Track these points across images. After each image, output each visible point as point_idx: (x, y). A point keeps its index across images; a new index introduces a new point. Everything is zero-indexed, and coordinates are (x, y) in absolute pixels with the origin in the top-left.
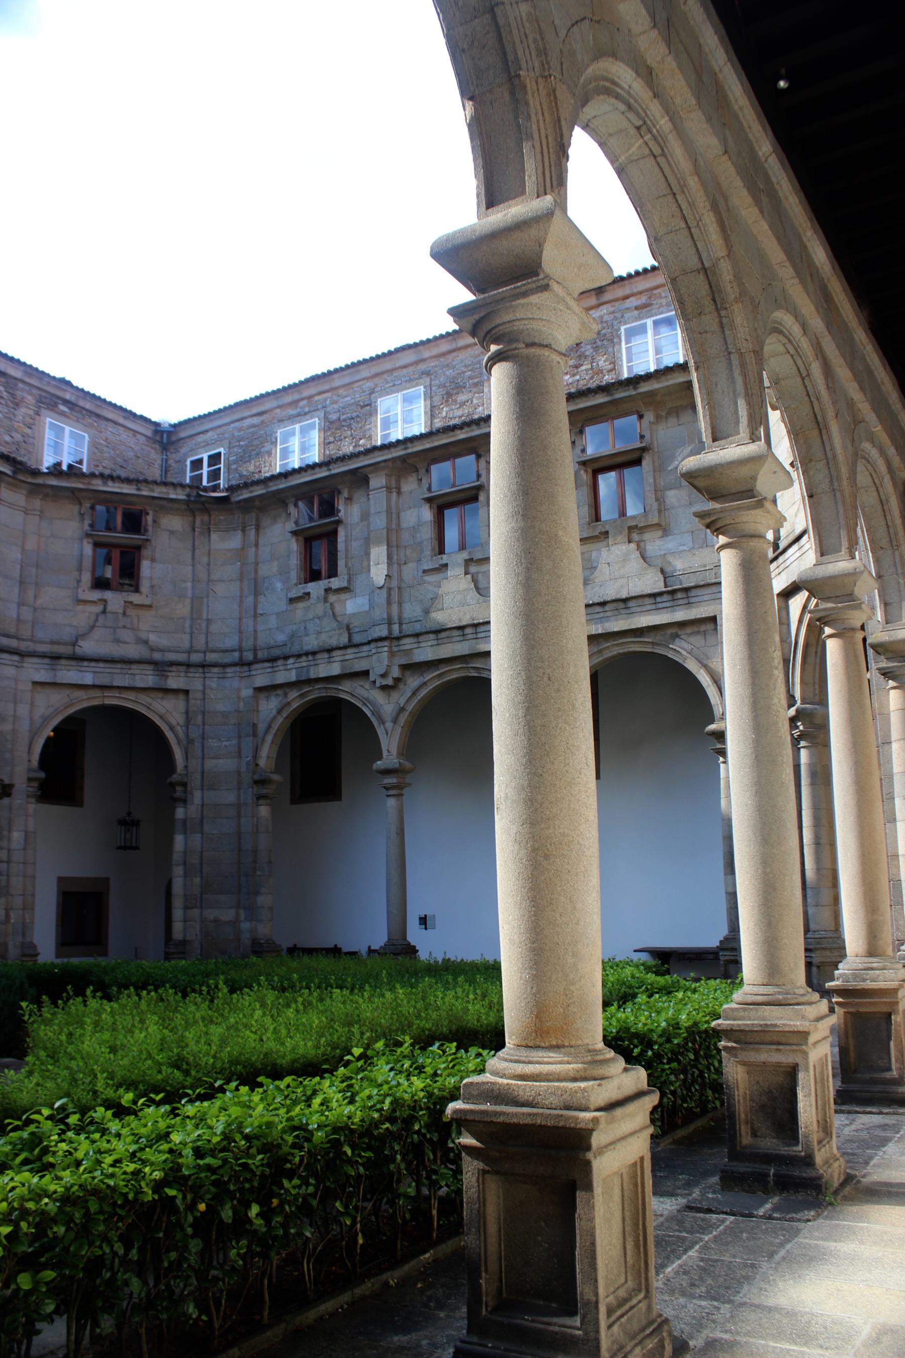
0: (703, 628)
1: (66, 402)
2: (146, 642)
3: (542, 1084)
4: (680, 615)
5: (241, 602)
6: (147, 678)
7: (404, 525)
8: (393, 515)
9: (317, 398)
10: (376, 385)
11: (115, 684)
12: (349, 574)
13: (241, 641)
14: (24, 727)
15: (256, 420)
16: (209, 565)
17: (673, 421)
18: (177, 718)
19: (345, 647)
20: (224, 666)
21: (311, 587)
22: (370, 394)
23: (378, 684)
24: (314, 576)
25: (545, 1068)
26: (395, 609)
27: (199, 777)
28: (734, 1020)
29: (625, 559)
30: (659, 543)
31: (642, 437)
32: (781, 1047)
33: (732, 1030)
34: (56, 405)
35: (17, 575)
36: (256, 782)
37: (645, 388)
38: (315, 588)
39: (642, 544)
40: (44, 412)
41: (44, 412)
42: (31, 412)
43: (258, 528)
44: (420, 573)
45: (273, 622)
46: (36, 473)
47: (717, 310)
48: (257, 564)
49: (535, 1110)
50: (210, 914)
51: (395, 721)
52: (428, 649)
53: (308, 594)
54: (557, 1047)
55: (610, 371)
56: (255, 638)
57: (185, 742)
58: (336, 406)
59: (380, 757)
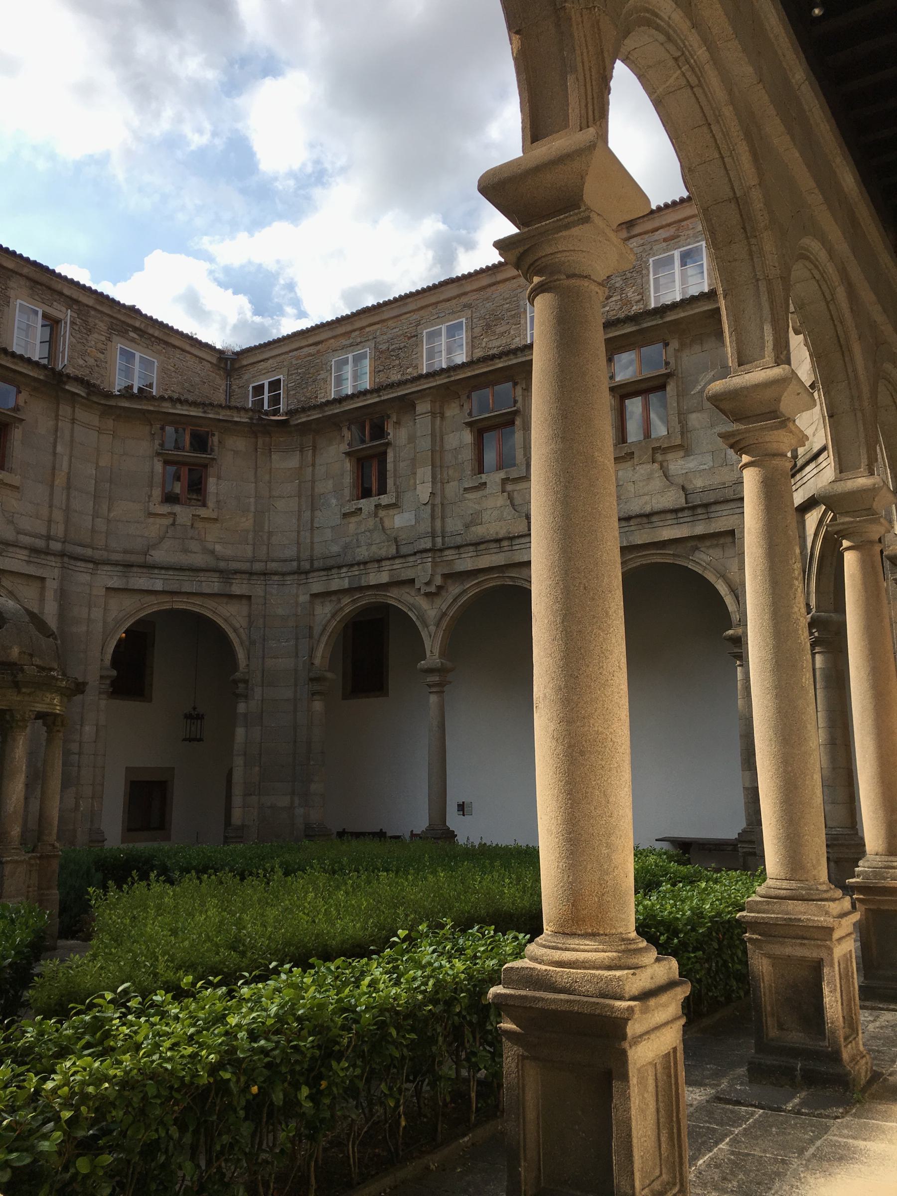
0: (722, 541)
1: (136, 329)
2: (212, 552)
3: (579, 971)
4: (700, 529)
5: (299, 516)
6: (213, 585)
7: (447, 447)
8: (437, 438)
9: (368, 329)
11: (183, 590)
12: (397, 492)
13: (299, 551)
15: (312, 350)
16: (270, 482)
17: (697, 348)
18: (240, 622)
20: (283, 574)
21: (364, 503)
22: (417, 326)
23: (422, 592)
24: (366, 493)
25: (581, 956)
26: (438, 523)
28: (758, 913)
29: (649, 478)
30: (681, 462)
31: (667, 364)
32: (806, 942)
33: (756, 922)
34: (127, 332)
35: (92, 489)
36: (312, 680)
37: (671, 317)
38: (367, 504)
39: (665, 464)
40: (115, 338)
41: (115, 338)
42: (103, 338)
43: (314, 448)
44: (461, 491)
45: (328, 534)
46: (109, 395)
47: (747, 238)
48: (313, 482)
49: (572, 997)
51: (438, 625)
52: (468, 560)
53: (361, 509)
54: (593, 935)
55: (639, 301)
56: (312, 549)
57: (247, 643)
58: (385, 337)
59: (424, 658)
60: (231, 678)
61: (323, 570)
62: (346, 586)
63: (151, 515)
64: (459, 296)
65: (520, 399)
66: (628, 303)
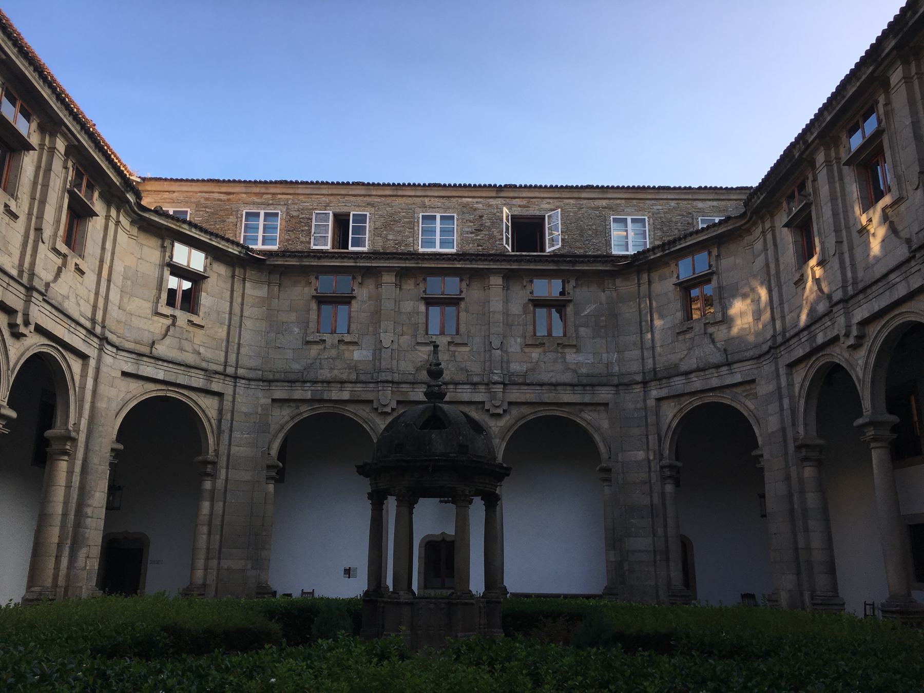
0: (598, 408)
2: (200, 354)
4: (587, 399)
6: (198, 380)
9: (280, 196)
10: (331, 202)
11: (178, 382)
14: (115, 406)
17: (585, 289)
18: (213, 414)
19: (356, 382)
20: (249, 380)
23: (380, 411)
27: (225, 458)
29: (555, 361)
30: (574, 356)
35: (120, 284)
36: (268, 467)
45: (289, 354)
50: (225, 564)
60: (200, 458)
61: (288, 382)
62: (309, 397)
63: (158, 314)
64: (365, 196)
65: (465, 291)
66: (492, 237)
